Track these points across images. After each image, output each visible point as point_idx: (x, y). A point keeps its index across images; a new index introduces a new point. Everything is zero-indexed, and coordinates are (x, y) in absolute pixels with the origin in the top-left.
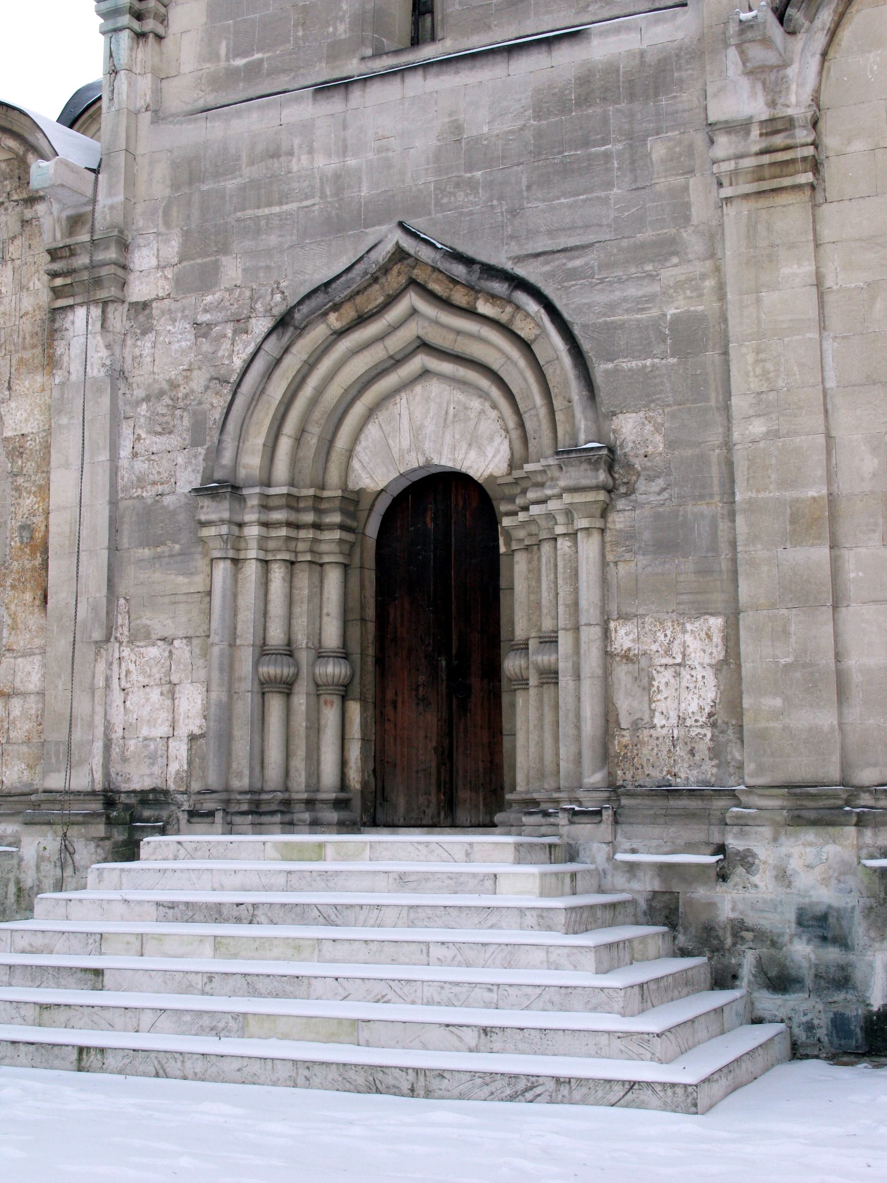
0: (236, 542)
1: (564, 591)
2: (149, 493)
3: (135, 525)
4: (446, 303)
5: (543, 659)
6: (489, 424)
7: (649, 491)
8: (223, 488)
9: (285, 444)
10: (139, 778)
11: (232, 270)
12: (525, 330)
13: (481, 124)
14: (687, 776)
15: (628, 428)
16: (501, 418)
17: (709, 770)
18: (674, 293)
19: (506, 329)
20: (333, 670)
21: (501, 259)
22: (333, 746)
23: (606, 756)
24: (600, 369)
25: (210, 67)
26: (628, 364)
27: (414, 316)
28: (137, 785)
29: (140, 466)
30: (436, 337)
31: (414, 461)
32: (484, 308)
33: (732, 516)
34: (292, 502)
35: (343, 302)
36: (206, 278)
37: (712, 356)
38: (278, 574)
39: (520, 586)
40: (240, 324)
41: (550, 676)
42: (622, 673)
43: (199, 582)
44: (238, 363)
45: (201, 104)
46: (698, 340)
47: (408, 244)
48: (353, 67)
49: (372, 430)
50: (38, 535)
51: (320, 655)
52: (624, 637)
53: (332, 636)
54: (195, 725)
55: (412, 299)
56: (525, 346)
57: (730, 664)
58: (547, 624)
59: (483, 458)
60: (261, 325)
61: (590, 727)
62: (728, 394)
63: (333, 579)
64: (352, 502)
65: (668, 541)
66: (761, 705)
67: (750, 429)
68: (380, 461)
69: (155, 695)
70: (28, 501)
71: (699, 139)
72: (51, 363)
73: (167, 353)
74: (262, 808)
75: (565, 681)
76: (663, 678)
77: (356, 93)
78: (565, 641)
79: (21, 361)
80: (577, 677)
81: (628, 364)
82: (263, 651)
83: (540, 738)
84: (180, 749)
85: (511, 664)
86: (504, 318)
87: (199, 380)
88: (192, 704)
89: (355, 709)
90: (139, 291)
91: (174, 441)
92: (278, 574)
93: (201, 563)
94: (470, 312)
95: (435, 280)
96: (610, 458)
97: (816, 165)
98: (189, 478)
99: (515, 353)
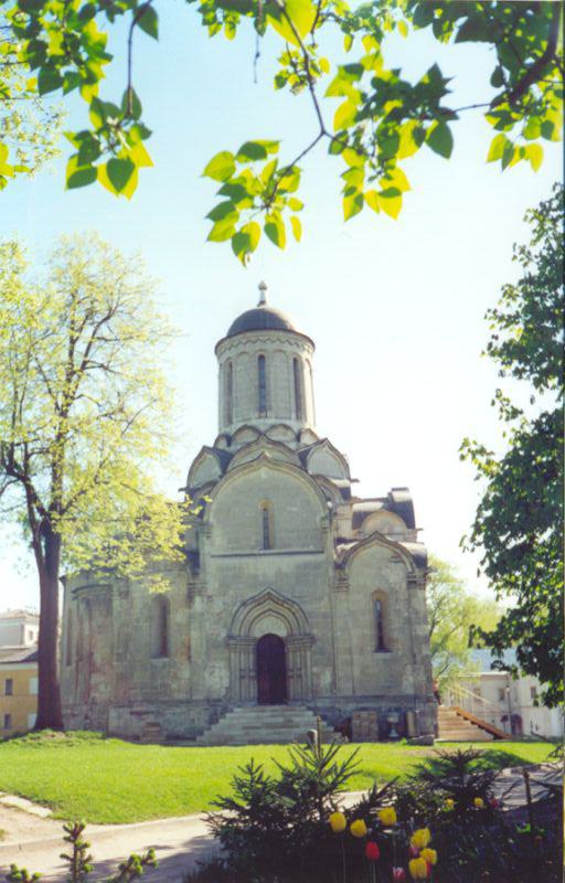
3: (212, 645)
7: (319, 643)
8: (230, 637)
10: (215, 696)
11: (231, 592)
12: (293, 610)
13: (285, 569)
15: (315, 631)
18: (323, 606)
22: (252, 689)
24: (310, 620)
27: (268, 605)
31: (267, 632)
35: (257, 601)
37: (329, 620)
41: (300, 676)
43: (227, 655)
46: (329, 617)
48: (256, 552)
52: (315, 669)
53: (251, 667)
54: (227, 685)
56: (294, 614)
57: (334, 674)
58: (299, 666)
59: (282, 632)
60: (239, 604)
64: (255, 639)
68: (258, 632)
70: (184, 637)
73: (218, 606)
74: (241, 703)
82: (241, 670)
83: (294, 687)
85: (290, 674)
88: (226, 682)
90: (210, 592)
95: (271, 598)
98: (223, 634)
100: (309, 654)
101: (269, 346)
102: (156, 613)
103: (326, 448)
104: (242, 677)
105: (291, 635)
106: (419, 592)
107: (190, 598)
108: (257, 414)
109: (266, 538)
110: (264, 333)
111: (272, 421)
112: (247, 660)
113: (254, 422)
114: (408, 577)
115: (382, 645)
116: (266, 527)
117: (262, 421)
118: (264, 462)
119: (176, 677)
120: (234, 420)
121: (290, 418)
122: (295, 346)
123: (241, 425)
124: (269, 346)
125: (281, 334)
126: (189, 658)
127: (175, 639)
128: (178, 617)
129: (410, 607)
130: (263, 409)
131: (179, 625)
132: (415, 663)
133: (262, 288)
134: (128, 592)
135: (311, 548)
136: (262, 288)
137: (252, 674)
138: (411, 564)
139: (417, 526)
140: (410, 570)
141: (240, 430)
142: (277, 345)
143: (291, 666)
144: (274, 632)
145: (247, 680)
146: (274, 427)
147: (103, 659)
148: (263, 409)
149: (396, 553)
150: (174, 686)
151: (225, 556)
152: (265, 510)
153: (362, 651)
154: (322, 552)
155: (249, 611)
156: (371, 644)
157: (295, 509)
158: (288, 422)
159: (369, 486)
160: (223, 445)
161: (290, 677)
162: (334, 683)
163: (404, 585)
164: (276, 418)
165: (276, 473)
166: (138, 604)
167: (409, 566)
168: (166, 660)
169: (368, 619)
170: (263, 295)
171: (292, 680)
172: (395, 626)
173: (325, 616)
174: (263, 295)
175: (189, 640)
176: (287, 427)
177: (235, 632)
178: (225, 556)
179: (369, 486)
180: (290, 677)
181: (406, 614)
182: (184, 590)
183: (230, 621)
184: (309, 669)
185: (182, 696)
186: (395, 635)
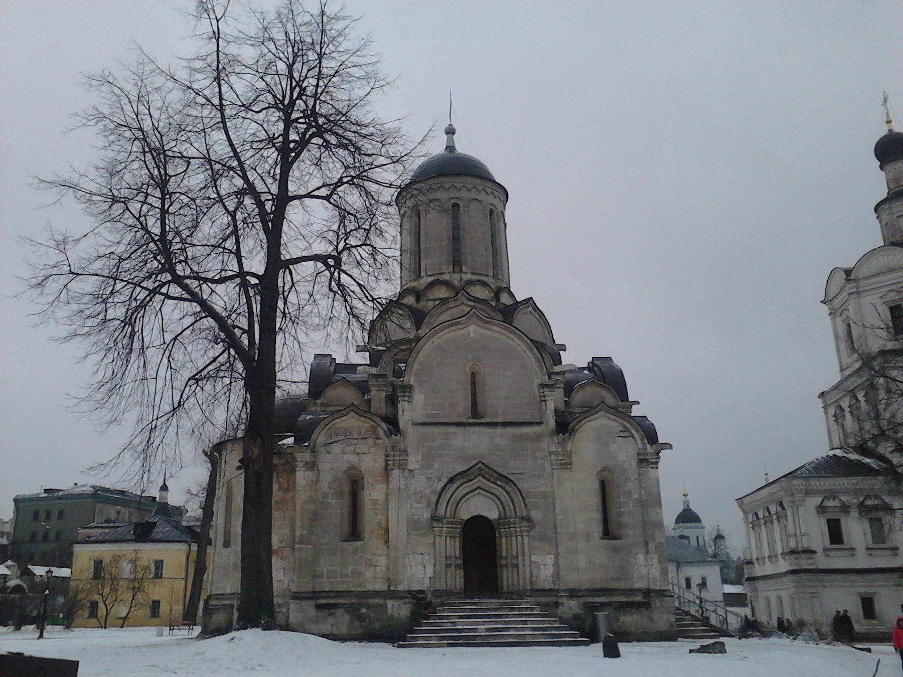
0: (441, 531)
1: (520, 547)
2: (416, 518)
3: (414, 525)
4: (489, 480)
5: (515, 562)
6: (494, 507)
7: (537, 527)
8: (435, 518)
9: (449, 508)
10: (416, 587)
11: (436, 465)
12: (508, 488)
14: (547, 587)
15: (533, 514)
16: (498, 506)
17: (552, 586)
19: (504, 489)
20: (460, 562)
21: (504, 473)
23: (531, 583)
24: (527, 501)
25: (425, 412)
26: (533, 500)
27: (480, 481)
28: (415, 589)
29: (413, 511)
30: (482, 486)
31: (476, 514)
32: (498, 483)
33: (556, 534)
34: (452, 523)
35: (464, 475)
36: (430, 466)
38: (448, 538)
39: (504, 545)
40: (440, 480)
42: (533, 566)
43: (431, 540)
44: (439, 488)
45: (423, 421)
47: (483, 467)
48: (464, 420)
49: (465, 505)
50: (383, 525)
51: (455, 557)
52: (534, 558)
53: (458, 554)
55: (480, 478)
56: (508, 493)
57: (556, 564)
59: (492, 514)
60: (445, 480)
61: (528, 577)
62: (555, 509)
63: (458, 539)
65: (543, 538)
66: (563, 573)
67: (559, 517)
68: (466, 512)
69: (420, 567)
71: (547, 454)
72: (388, 483)
73: (419, 483)
75: (520, 566)
76: (542, 567)
77: (467, 428)
78: (520, 559)
79: (376, 480)
80: (524, 566)
81: (533, 500)
83: (507, 579)
84: (427, 581)
86: (503, 485)
87: (428, 492)
89: (462, 571)
90: (410, 467)
91: (421, 505)
92: (448, 538)
93: (432, 537)
94: (495, 483)
96: (529, 520)
97: (570, 464)
98: (427, 515)
99: (505, 493)
100: (526, 539)
101: (464, 194)
102: (346, 488)
103: (531, 309)
104: (448, 566)
105: (503, 517)
106: (652, 472)
107: (387, 470)
108: (451, 269)
109: (474, 404)
110: (459, 179)
111: (467, 277)
112: (453, 547)
113: (446, 277)
114: (638, 454)
115: (608, 532)
116: (474, 394)
117: (456, 276)
118: (475, 319)
119: (370, 564)
120: (423, 274)
121: (488, 276)
122: (491, 196)
123: (430, 279)
124: (464, 194)
125: (477, 181)
126: (387, 542)
127: (370, 519)
128: (373, 493)
129: (641, 487)
130: (457, 264)
131: (375, 502)
132: (648, 552)
133: (450, 131)
134: (314, 462)
135: (528, 418)
136: (450, 131)
137: (460, 562)
138: (642, 440)
139: (631, 398)
140: (640, 446)
141: (431, 285)
142: (473, 194)
143: (504, 554)
144: (483, 514)
145: (453, 569)
146: (471, 283)
147: (281, 542)
148: (457, 264)
149: (624, 426)
150: (368, 574)
151: (424, 424)
152: (473, 373)
153: (588, 537)
154: (540, 423)
155: (457, 488)
156: (597, 529)
157: (510, 374)
158: (485, 279)
159: (575, 357)
160: (410, 300)
161: (502, 566)
162: (556, 575)
163: (634, 463)
164: (472, 274)
165: (488, 332)
166: (326, 479)
167: (639, 441)
168: (358, 543)
169: (595, 500)
170: (450, 140)
171: (505, 570)
172: (627, 510)
173: (545, 495)
174: (450, 140)
175: (387, 521)
176: (484, 284)
177: (441, 511)
178: (424, 424)
179: (575, 357)
180: (502, 566)
181: (636, 496)
182: (381, 462)
183: (434, 499)
184: (527, 558)
185: (379, 586)
186: (625, 519)
